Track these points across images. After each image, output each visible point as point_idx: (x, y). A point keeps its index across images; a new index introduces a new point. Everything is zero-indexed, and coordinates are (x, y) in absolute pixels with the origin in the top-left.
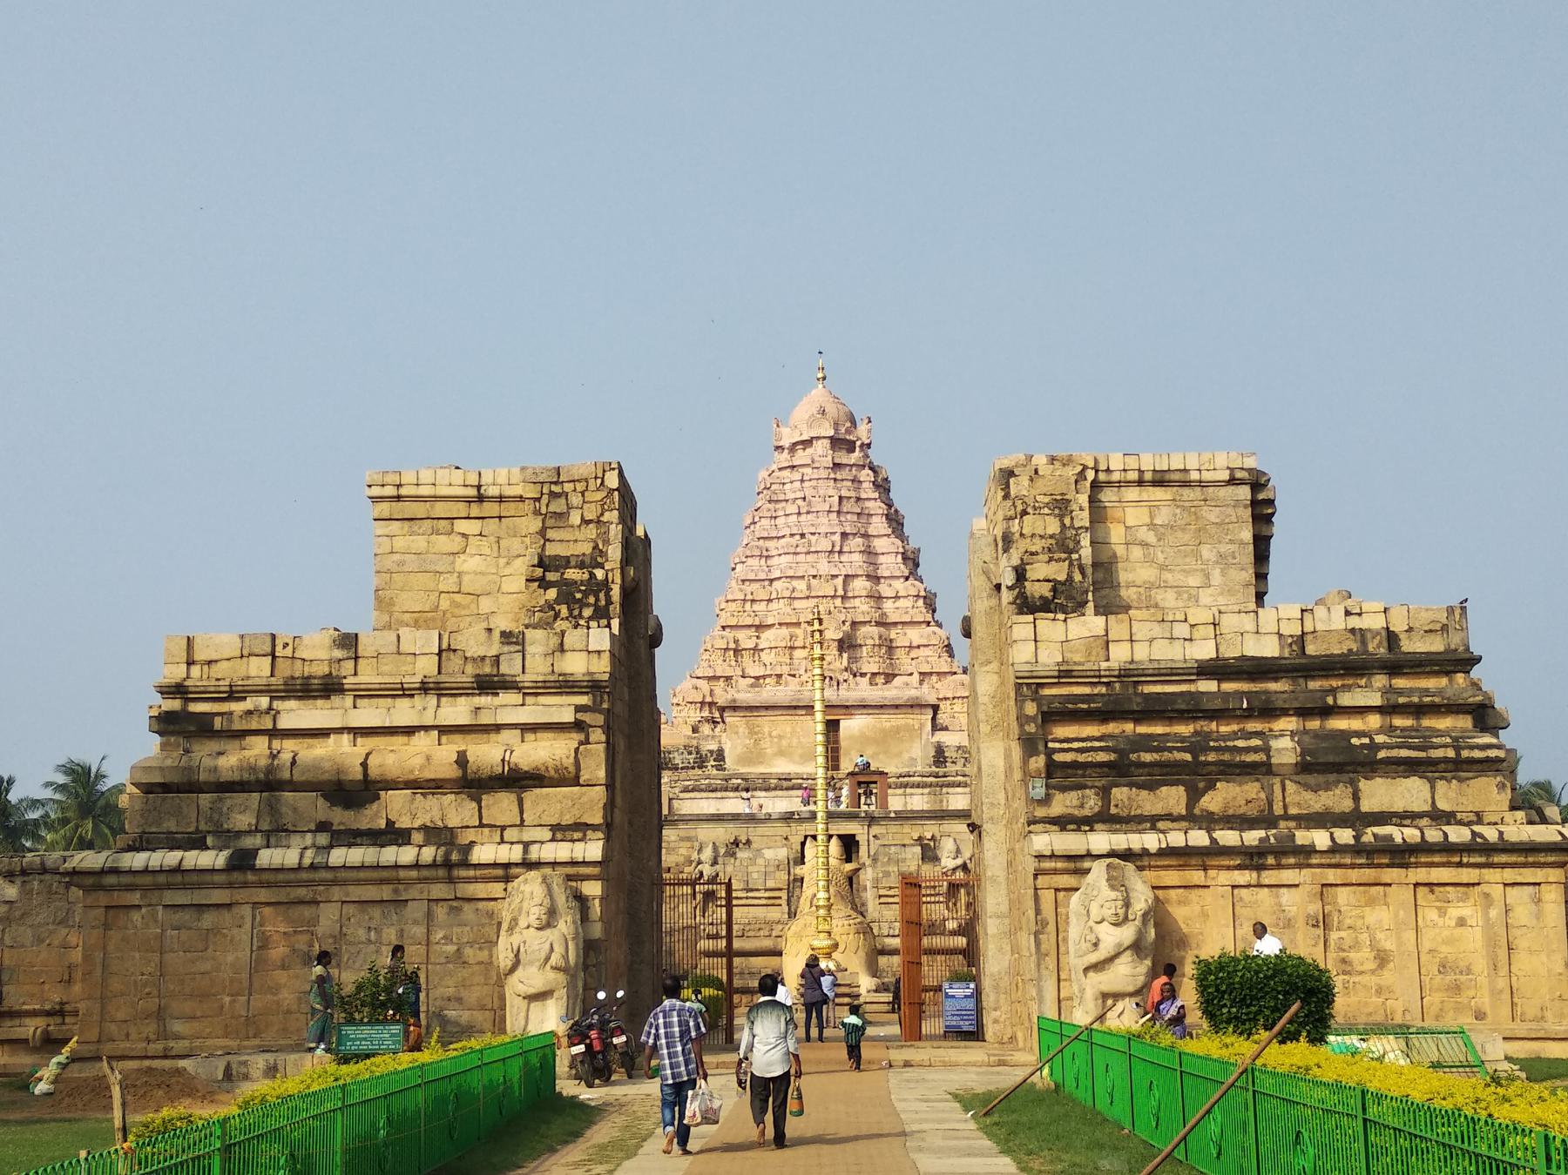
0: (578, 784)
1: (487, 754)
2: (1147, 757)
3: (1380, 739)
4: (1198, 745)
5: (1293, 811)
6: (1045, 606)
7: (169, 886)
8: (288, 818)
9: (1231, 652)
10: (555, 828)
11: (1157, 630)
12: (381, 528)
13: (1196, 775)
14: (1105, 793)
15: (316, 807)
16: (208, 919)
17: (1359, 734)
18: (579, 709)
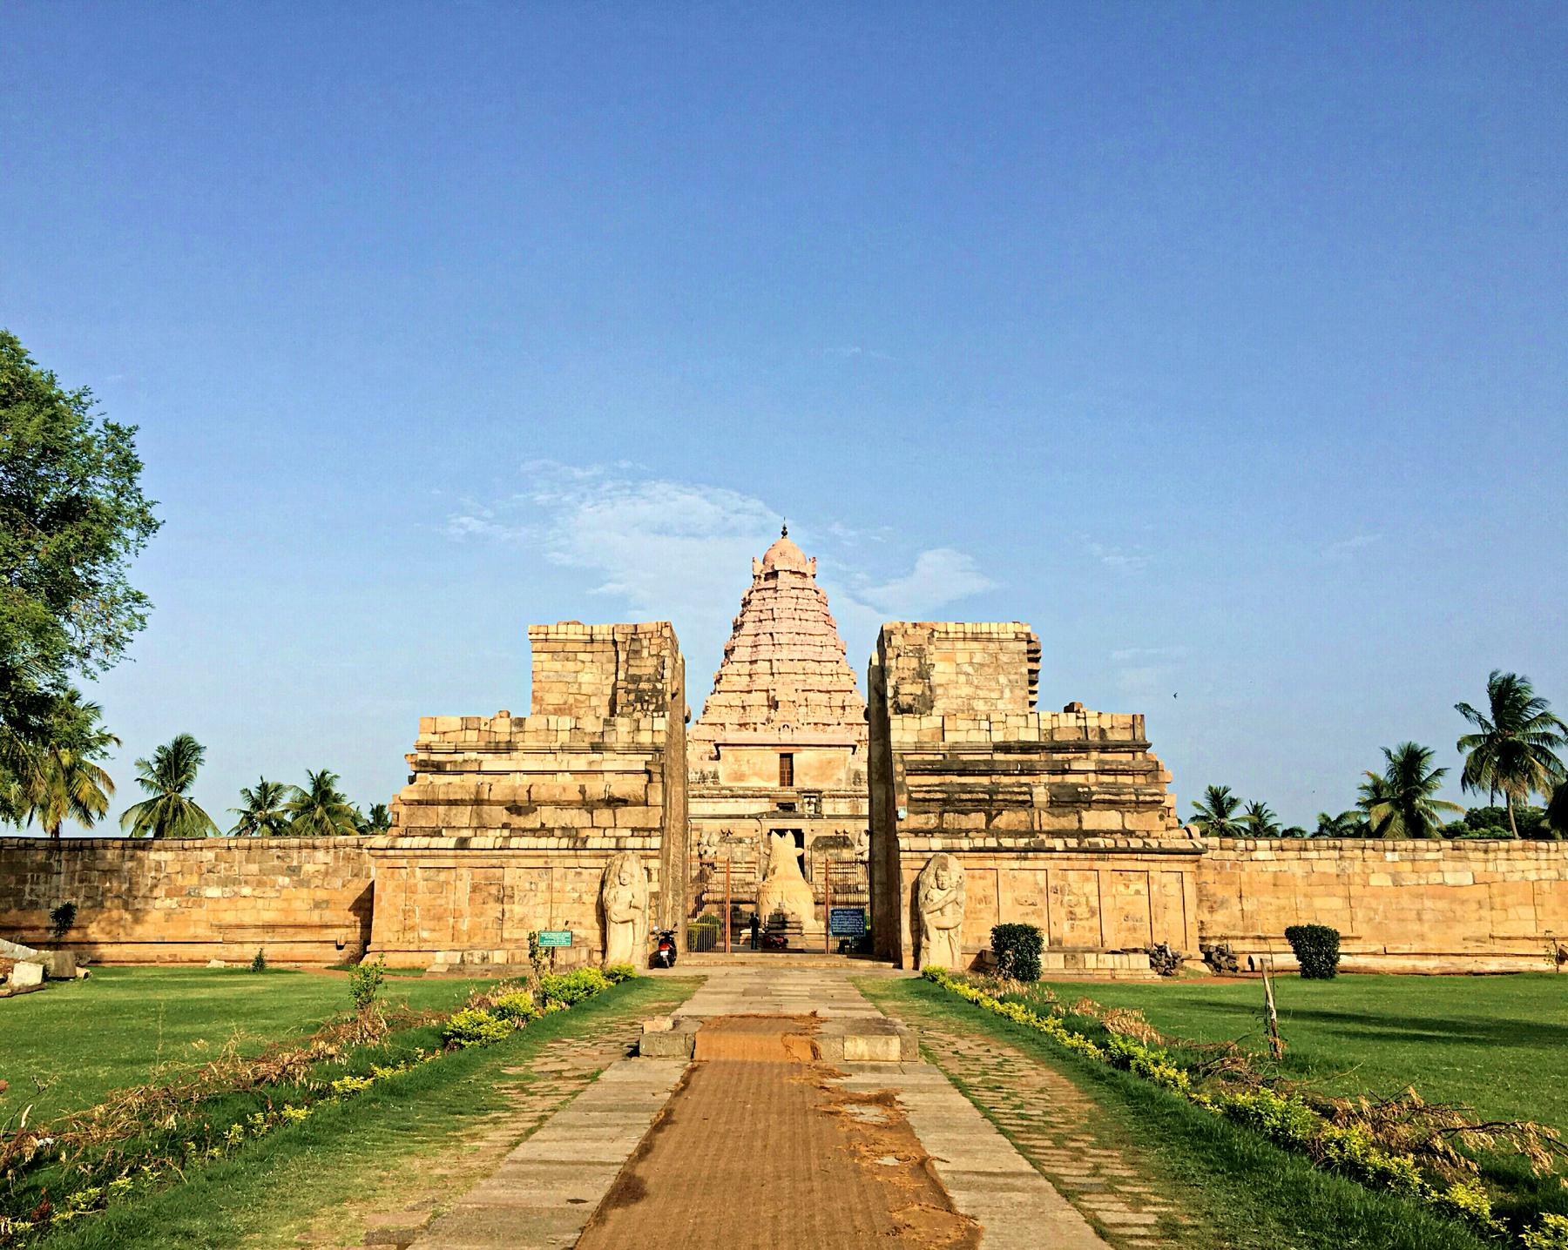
0: (646, 804)
1: (596, 787)
2: (965, 796)
3: (1094, 789)
4: (992, 791)
5: (1045, 828)
6: (909, 710)
7: (422, 857)
8: (487, 821)
9: (1012, 739)
10: (633, 830)
11: (971, 724)
12: (535, 657)
13: (990, 805)
14: (941, 815)
15: (502, 815)
16: (443, 876)
17: (1083, 786)
18: (646, 763)
